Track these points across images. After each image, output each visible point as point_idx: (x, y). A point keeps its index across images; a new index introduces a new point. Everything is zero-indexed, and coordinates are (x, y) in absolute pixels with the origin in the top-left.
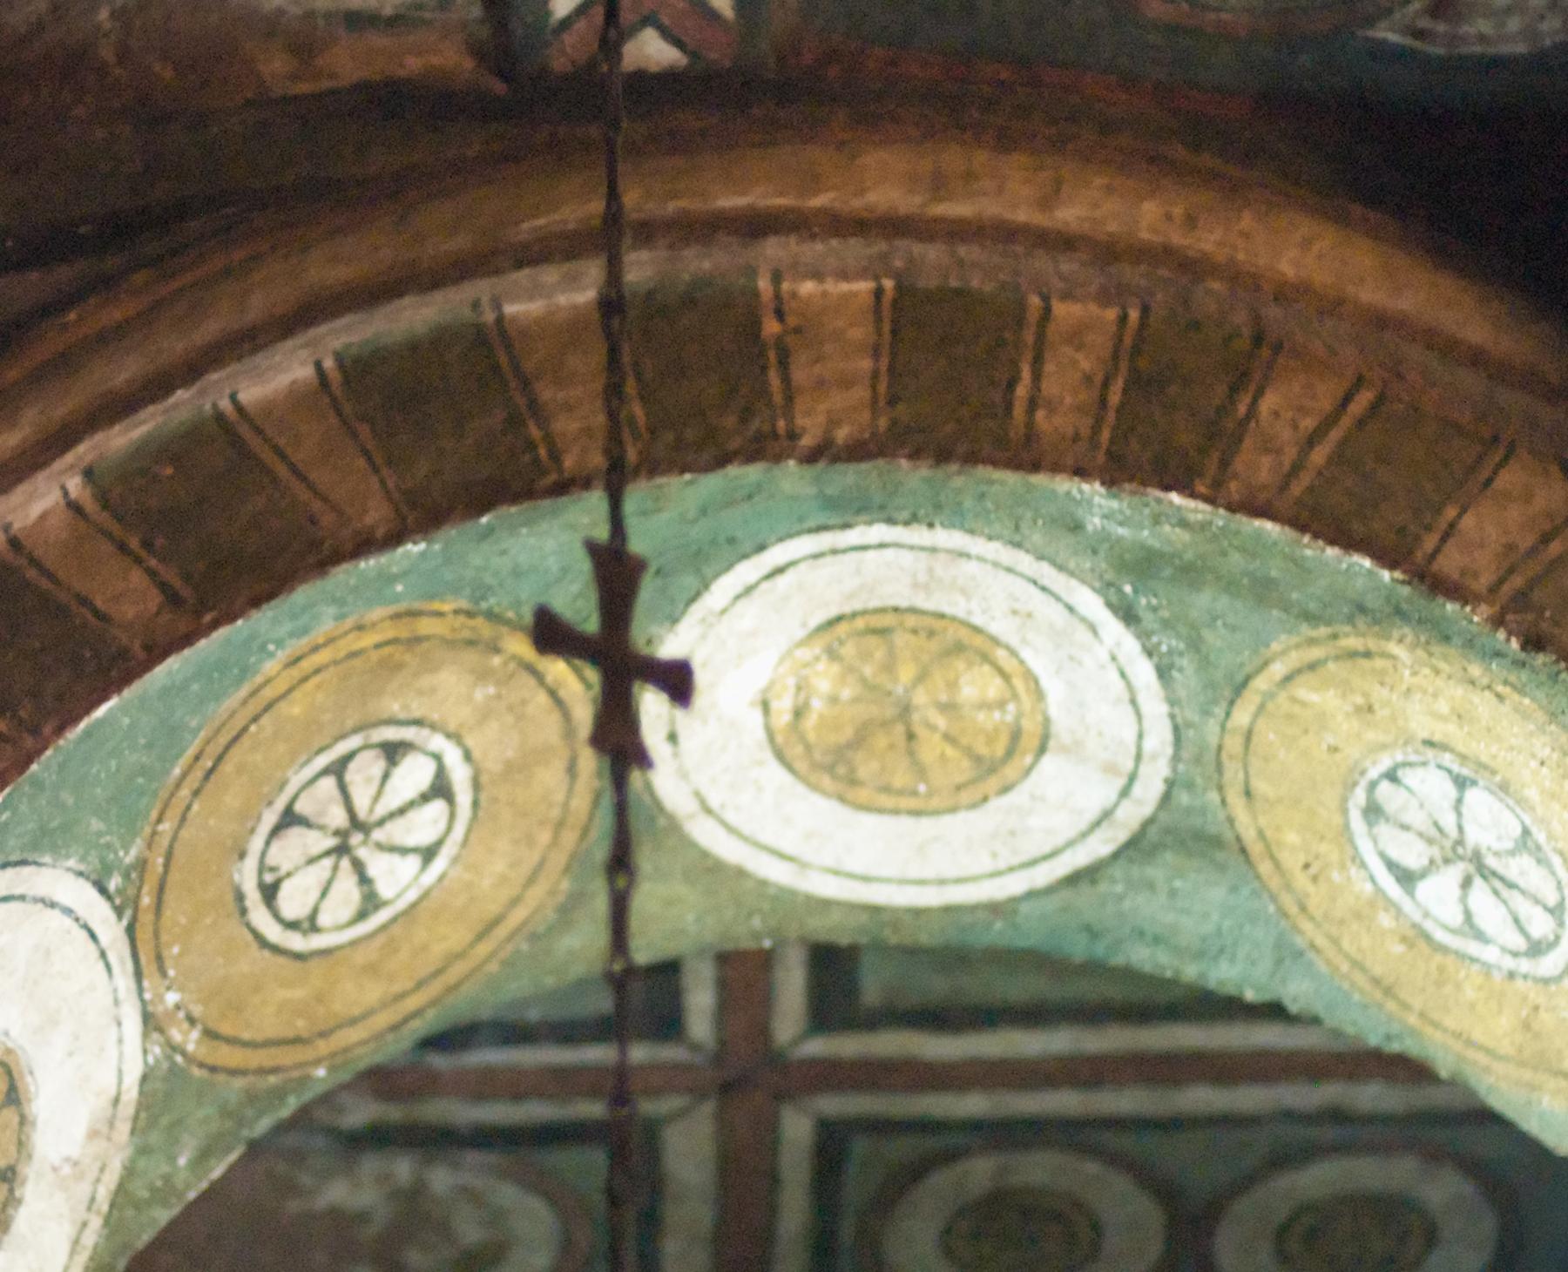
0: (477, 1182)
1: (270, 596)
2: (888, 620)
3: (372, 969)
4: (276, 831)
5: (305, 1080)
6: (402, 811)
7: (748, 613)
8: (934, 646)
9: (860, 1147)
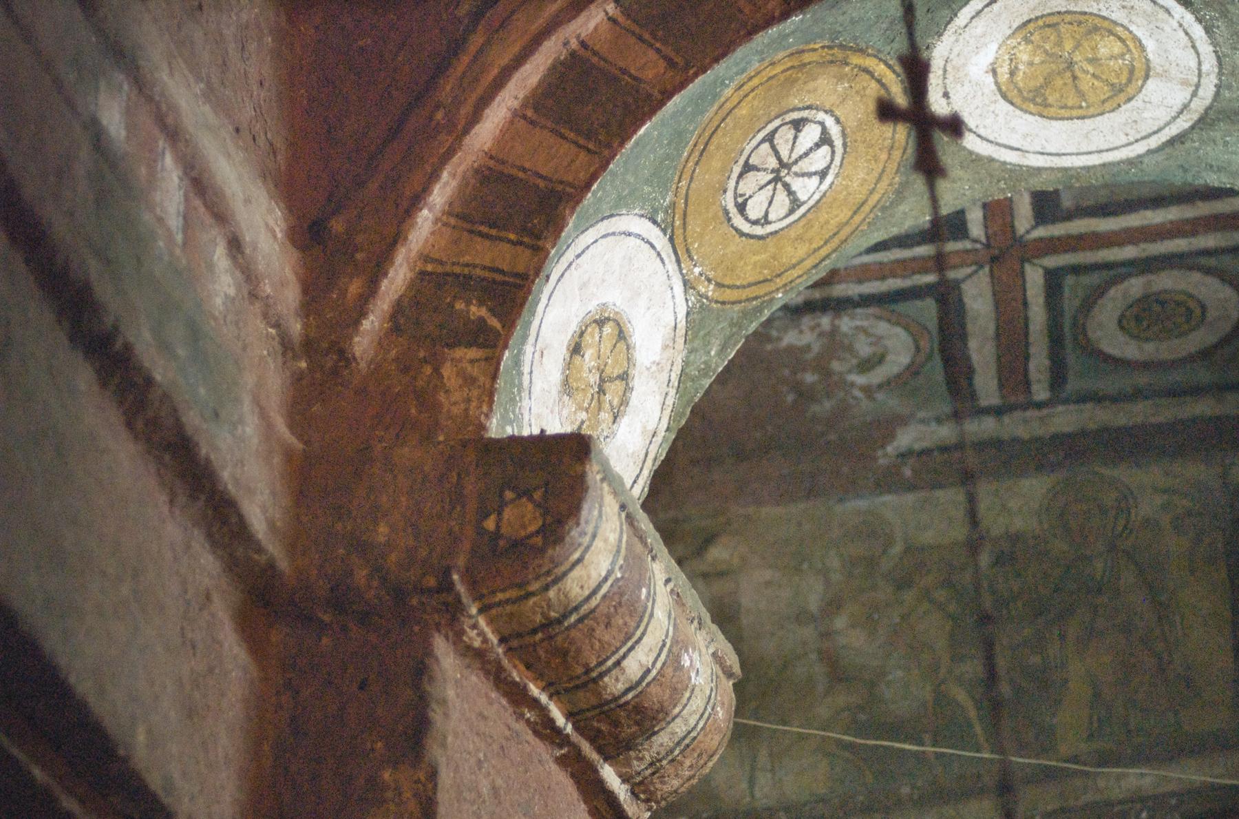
0: (865, 323)
1: (724, 55)
2: (1055, 19)
3: (799, 238)
4: (741, 176)
5: (772, 300)
6: (806, 154)
7: (980, 26)
8: (1082, 30)
9: (1070, 280)
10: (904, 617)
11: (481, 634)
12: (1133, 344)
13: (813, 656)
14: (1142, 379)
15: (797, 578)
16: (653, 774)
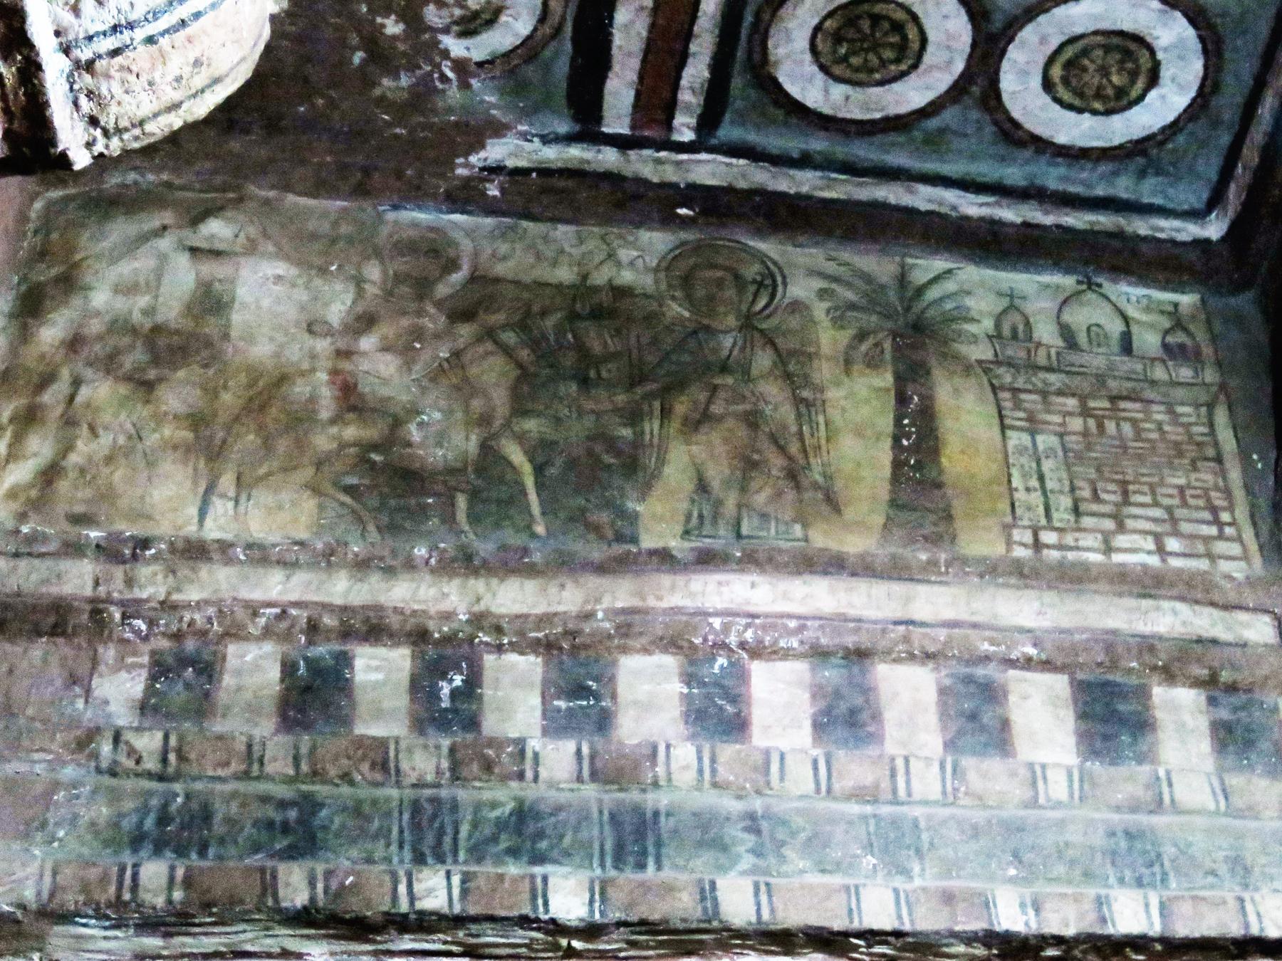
10: (457, 354)
12: (820, 77)
13: (323, 376)
14: (818, 144)
15: (318, 282)
16: (115, 53)
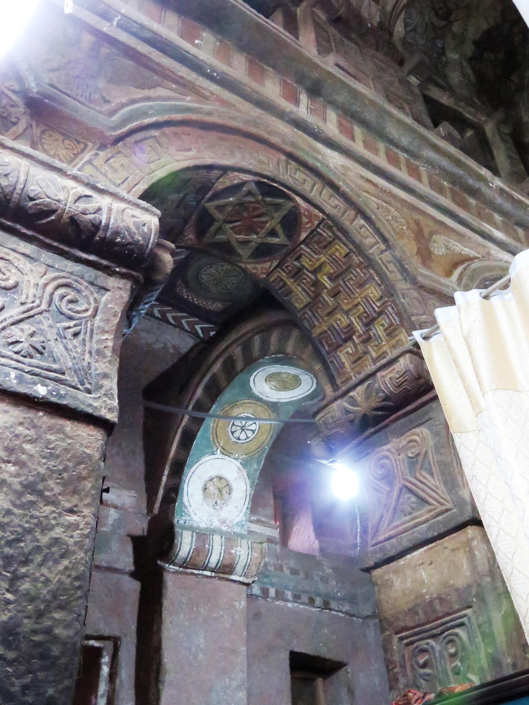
11: (173, 569)
